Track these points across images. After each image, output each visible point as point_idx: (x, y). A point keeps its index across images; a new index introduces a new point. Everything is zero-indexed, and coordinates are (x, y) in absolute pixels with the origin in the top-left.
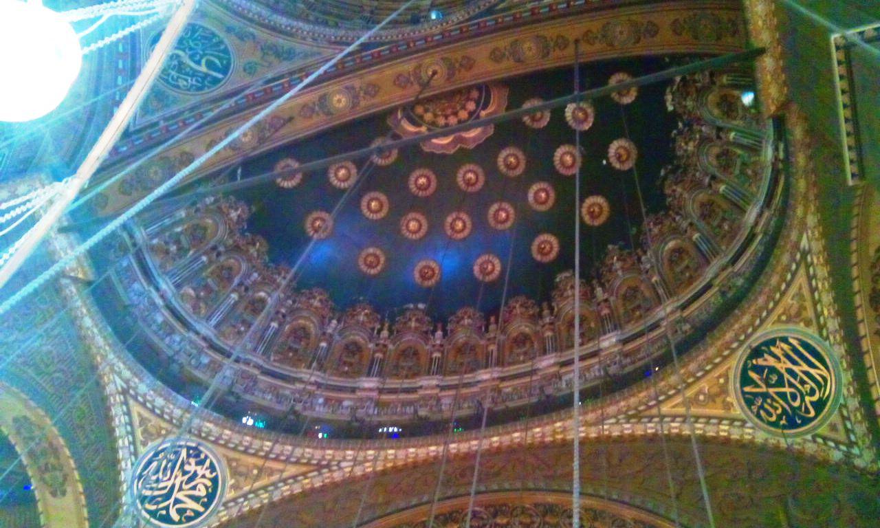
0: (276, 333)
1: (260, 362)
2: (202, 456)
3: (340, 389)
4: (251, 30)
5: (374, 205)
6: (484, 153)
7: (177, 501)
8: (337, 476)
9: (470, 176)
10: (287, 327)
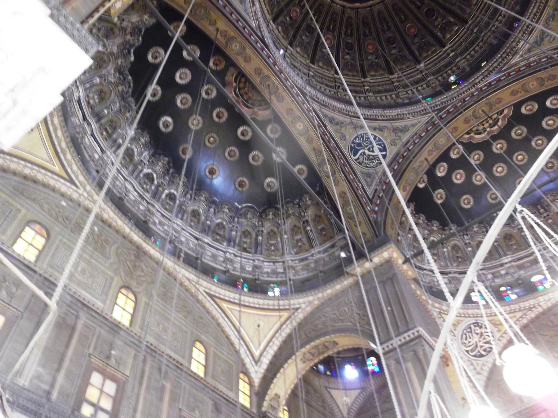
0: (448, 251)
1: (455, 270)
2: (480, 324)
3: (496, 267)
4: (384, 124)
5: (458, 178)
6: (504, 134)
7: (481, 347)
8: (540, 310)
9: (499, 146)
10: (449, 248)
